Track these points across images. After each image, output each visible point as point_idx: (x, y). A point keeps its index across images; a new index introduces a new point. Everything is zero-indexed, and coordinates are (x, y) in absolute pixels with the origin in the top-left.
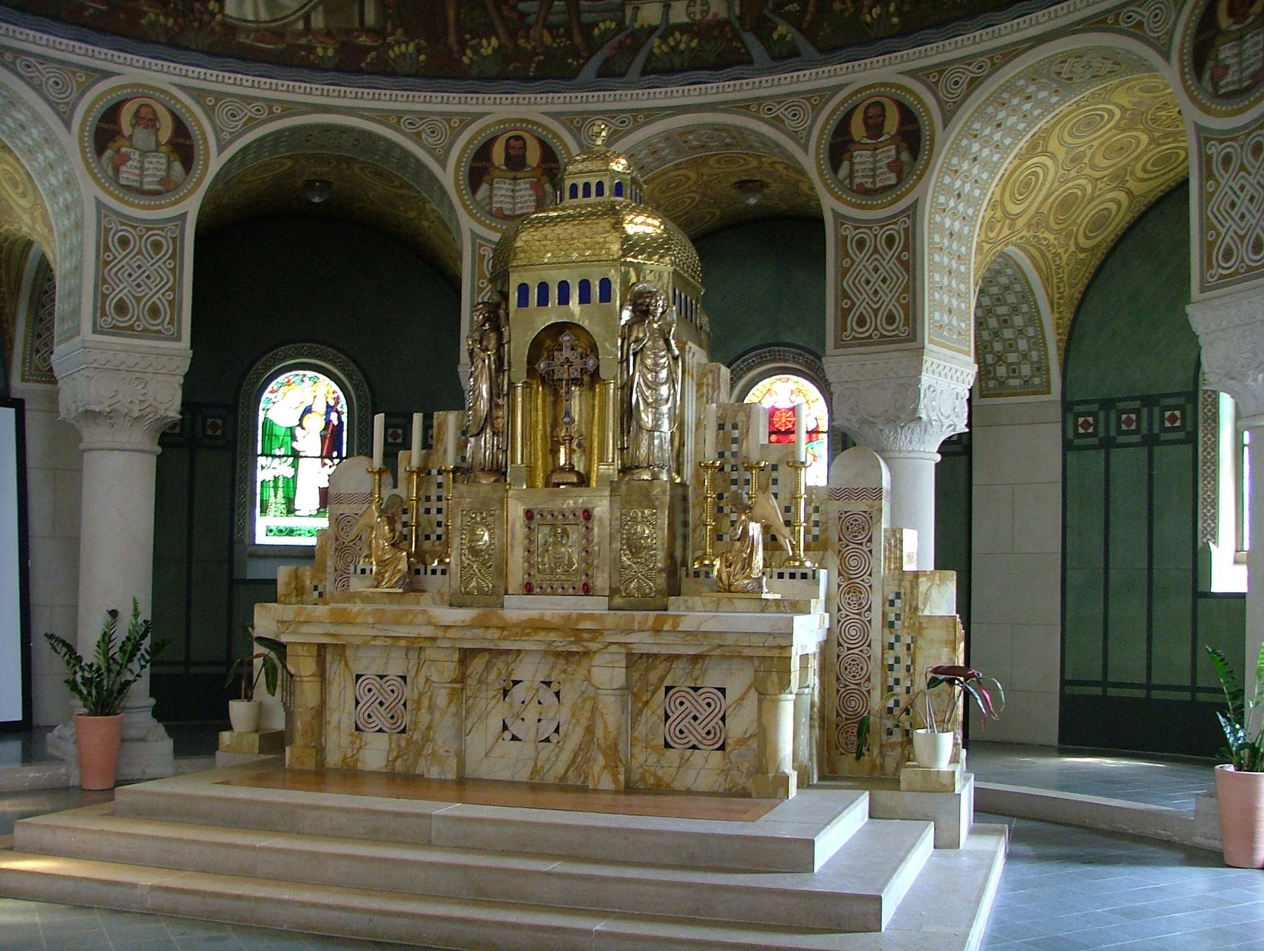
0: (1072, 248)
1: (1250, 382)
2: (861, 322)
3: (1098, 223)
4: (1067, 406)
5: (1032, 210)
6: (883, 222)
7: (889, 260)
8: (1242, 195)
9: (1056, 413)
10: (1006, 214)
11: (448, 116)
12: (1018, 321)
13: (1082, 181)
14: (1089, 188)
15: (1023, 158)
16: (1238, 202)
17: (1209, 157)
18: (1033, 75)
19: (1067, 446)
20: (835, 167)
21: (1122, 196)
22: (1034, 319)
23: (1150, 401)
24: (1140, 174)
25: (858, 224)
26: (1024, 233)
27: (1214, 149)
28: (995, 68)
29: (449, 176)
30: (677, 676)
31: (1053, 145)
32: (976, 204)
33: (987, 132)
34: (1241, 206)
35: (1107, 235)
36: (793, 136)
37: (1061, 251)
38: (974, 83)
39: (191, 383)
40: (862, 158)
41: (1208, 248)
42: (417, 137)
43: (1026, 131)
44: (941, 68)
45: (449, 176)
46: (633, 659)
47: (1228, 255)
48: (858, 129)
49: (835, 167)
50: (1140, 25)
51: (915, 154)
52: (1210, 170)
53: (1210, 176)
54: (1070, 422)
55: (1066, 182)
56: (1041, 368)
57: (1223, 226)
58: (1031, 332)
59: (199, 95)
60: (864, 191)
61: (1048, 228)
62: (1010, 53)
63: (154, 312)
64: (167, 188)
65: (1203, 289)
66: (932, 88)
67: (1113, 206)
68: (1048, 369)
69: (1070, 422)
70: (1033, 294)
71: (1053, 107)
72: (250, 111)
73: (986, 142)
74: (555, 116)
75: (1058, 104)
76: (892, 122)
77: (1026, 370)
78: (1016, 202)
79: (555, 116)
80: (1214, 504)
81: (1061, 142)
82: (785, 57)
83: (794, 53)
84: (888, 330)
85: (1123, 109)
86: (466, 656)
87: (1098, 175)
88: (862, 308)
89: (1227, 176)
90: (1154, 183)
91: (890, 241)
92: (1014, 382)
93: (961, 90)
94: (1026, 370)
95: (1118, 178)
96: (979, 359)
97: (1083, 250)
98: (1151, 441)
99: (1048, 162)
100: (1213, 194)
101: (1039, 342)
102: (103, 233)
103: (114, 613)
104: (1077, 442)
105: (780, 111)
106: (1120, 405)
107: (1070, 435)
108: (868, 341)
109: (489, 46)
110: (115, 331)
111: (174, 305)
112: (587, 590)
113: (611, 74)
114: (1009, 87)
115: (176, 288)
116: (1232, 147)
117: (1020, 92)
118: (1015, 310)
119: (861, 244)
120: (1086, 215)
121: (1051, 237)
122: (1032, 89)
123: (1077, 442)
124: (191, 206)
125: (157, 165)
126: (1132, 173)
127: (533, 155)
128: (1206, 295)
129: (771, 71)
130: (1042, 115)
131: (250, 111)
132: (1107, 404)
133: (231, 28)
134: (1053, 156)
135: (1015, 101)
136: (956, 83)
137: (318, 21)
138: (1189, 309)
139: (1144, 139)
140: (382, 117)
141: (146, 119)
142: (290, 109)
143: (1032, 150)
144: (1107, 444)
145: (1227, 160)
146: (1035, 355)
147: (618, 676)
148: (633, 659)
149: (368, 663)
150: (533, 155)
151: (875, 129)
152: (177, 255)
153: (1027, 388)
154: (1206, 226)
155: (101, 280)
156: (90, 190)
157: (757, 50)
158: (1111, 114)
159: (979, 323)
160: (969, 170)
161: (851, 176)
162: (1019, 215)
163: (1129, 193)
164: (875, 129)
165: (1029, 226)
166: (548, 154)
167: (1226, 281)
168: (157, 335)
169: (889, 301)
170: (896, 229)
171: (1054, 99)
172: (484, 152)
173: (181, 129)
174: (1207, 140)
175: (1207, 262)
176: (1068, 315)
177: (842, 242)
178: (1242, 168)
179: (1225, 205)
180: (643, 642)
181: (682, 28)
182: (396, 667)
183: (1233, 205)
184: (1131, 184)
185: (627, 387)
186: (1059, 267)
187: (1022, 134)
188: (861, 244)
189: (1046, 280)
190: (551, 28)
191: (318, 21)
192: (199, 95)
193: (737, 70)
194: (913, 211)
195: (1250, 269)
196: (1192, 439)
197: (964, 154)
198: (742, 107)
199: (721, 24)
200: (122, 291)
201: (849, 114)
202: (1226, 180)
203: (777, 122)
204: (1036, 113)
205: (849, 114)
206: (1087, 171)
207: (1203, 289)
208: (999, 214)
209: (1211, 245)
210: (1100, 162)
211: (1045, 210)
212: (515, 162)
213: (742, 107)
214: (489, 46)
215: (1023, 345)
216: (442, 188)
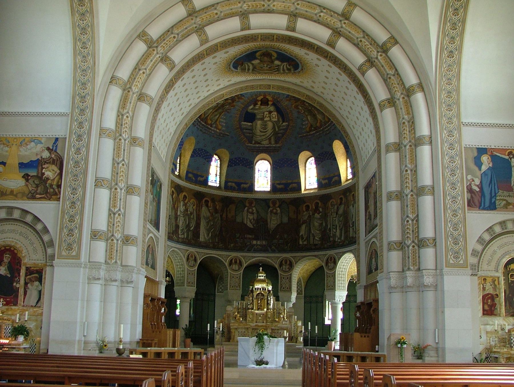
2: (283, 288)
4: (305, 297)
6: (287, 275)
7: (287, 281)
11: (227, 255)
19: (305, 303)
20: (280, 267)
23: (317, 296)
25: (283, 275)
29: (227, 264)
30: (276, 331)
35: (311, 273)
36: (274, 262)
38: (299, 260)
39: (197, 293)
40: (284, 267)
42: (223, 258)
44: (295, 256)
45: (227, 264)
46: (272, 329)
48: (283, 262)
49: (280, 267)
51: (291, 267)
59: (197, 252)
60: (284, 271)
62: (305, 257)
63: (192, 283)
64: (194, 266)
66: (294, 259)
72: (203, 254)
74: (241, 256)
76: (288, 262)
79: (241, 256)
80: (326, 312)
82: (273, 251)
83: (275, 251)
84: (287, 290)
86: (253, 329)
88: (284, 286)
91: (288, 278)
95: (314, 267)
98: (317, 302)
102: (188, 272)
103: (186, 325)
105: (272, 258)
108: (284, 291)
109: (232, 245)
110: (189, 286)
111: (194, 282)
112: (263, 322)
113: (249, 251)
115: (195, 280)
119: (284, 278)
120: (309, 271)
124: (196, 268)
125: (193, 262)
127: (238, 262)
129: (272, 253)
131: (203, 254)
132: (311, 297)
133: (201, 242)
137: (210, 241)
140: (218, 255)
141: (192, 256)
142: (207, 254)
144: (311, 303)
145: (329, 276)
147: (271, 331)
148: (272, 329)
149: (240, 330)
150: (238, 262)
151: (286, 263)
152: (195, 275)
155: (187, 279)
156: (186, 266)
157: (270, 250)
159: (297, 288)
161: (282, 269)
164: (286, 263)
166: (240, 262)
168: (192, 286)
169: (287, 286)
170: (289, 277)
172: (231, 261)
173: (195, 257)
177: (281, 278)
180: (273, 328)
181: (259, 245)
182: (244, 330)
185: (268, 300)
188: (284, 278)
189: (303, 279)
190: (241, 243)
191: (210, 241)
192: (197, 252)
193: (266, 252)
194: (291, 274)
198: (267, 257)
199: (265, 245)
200: (189, 281)
201: (282, 261)
203: (272, 260)
205: (282, 261)
212: (236, 262)
213: (267, 257)
214: (232, 245)
216: (225, 265)
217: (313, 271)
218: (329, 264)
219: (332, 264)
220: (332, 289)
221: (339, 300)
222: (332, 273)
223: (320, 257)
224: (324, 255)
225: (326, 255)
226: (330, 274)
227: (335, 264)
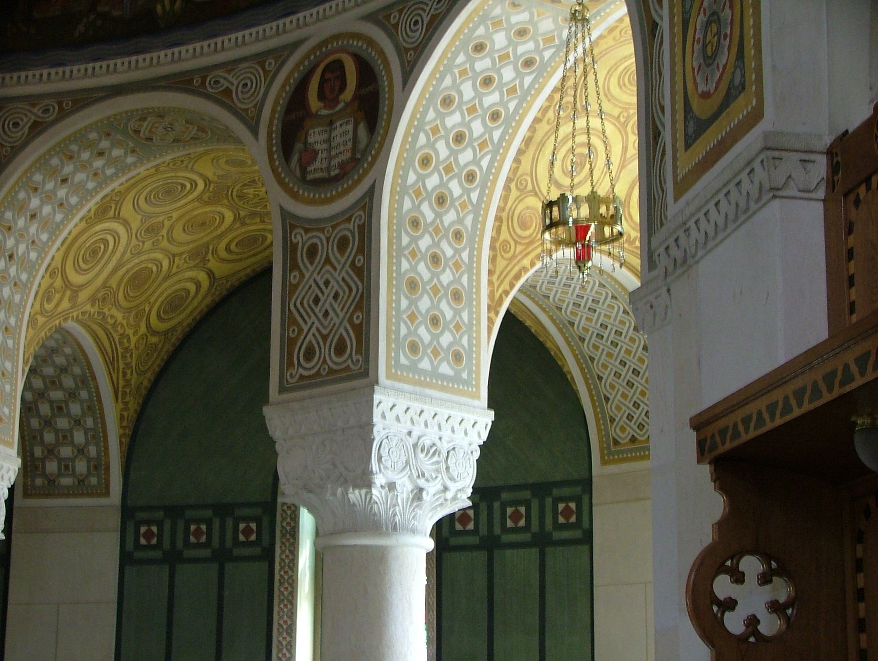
0: (143, 329)
1: (328, 496)
3: (174, 303)
4: (127, 512)
5: (100, 281)
8: (326, 292)
9: (115, 520)
10: (67, 284)
12: (75, 409)
13: (159, 256)
14: (166, 264)
15: (90, 221)
16: (322, 299)
17: (294, 247)
18: (108, 129)
19: (126, 559)
21: (202, 277)
22: (94, 407)
23: (223, 510)
24: (223, 254)
26: (88, 307)
27: (299, 238)
28: (63, 115)
31: (127, 210)
32: (32, 268)
33: (50, 186)
34: (326, 301)
35: (183, 318)
37: (130, 332)
38: (38, 128)
41: (289, 344)
43: (96, 190)
47: (309, 354)
50: (227, 92)
52: (294, 259)
53: (295, 266)
54: (131, 529)
55: (139, 253)
56: (100, 466)
57: (306, 322)
58: (90, 422)
61: (116, 304)
65: (283, 389)
67: (192, 288)
68: (107, 468)
69: (131, 529)
70: (94, 378)
71: (129, 168)
73: (49, 197)
75: (135, 164)
77: (81, 467)
78: (79, 271)
80: (291, 630)
81: (136, 206)
85: (207, 182)
87: (175, 249)
89: (311, 268)
90: (237, 266)
92: (66, 481)
93: (19, 135)
94: (81, 467)
95: (200, 255)
96: (25, 452)
97: (154, 333)
99: (121, 230)
100: (296, 287)
101: (99, 435)
104: (139, 555)
106: (189, 513)
107: (130, 546)
114: (79, 137)
116: (318, 238)
117: (91, 145)
118: (72, 395)
120: (161, 293)
121: (119, 316)
122: (105, 144)
123: (139, 555)
126: (215, 252)
128: (286, 396)
130: (116, 175)
132: (174, 511)
134: (126, 223)
135: (85, 155)
136: (16, 124)
138: (267, 411)
139: (229, 216)
143: (102, 213)
145: (312, 252)
146: (93, 450)
153: (81, 488)
154: (288, 320)
158: (194, 184)
160: (26, 228)
162: (82, 287)
163: (210, 274)
165: (93, 300)
167: (308, 382)
171: (130, 160)
174: (293, 227)
175: (287, 361)
176: (134, 406)
178: (328, 261)
179: (309, 300)
183: (317, 300)
184: (213, 264)
186: (126, 349)
187: (90, 194)
189: (111, 363)
195: (331, 371)
196: (269, 555)
197: (21, 208)
202: (311, 272)
204: (109, 172)
206: (165, 243)
207: (282, 389)
208: (58, 282)
209: (292, 342)
210: (179, 234)
211: (113, 283)
215: (79, 437)
217: (197, 304)
218: (316, 136)
219: (343, 132)
220: (336, 375)
221: (405, 487)
222: (346, 216)
223: (232, 80)
224: (260, 58)
225: (281, 53)
226: (310, 226)
227: (372, 128)
